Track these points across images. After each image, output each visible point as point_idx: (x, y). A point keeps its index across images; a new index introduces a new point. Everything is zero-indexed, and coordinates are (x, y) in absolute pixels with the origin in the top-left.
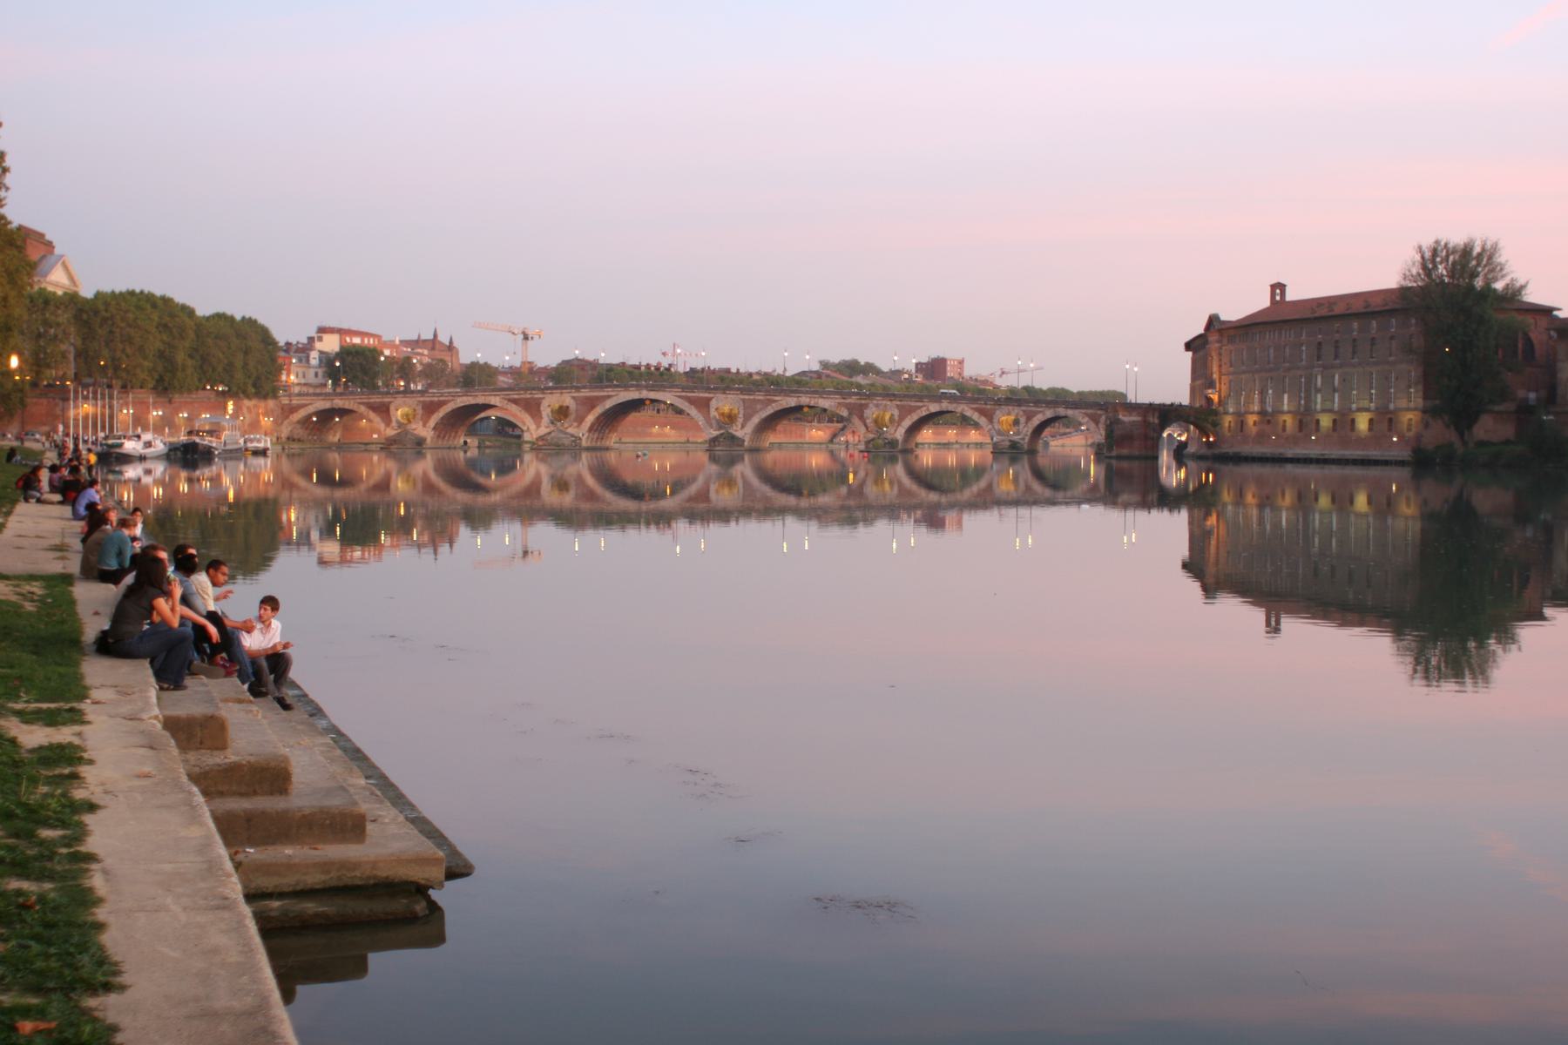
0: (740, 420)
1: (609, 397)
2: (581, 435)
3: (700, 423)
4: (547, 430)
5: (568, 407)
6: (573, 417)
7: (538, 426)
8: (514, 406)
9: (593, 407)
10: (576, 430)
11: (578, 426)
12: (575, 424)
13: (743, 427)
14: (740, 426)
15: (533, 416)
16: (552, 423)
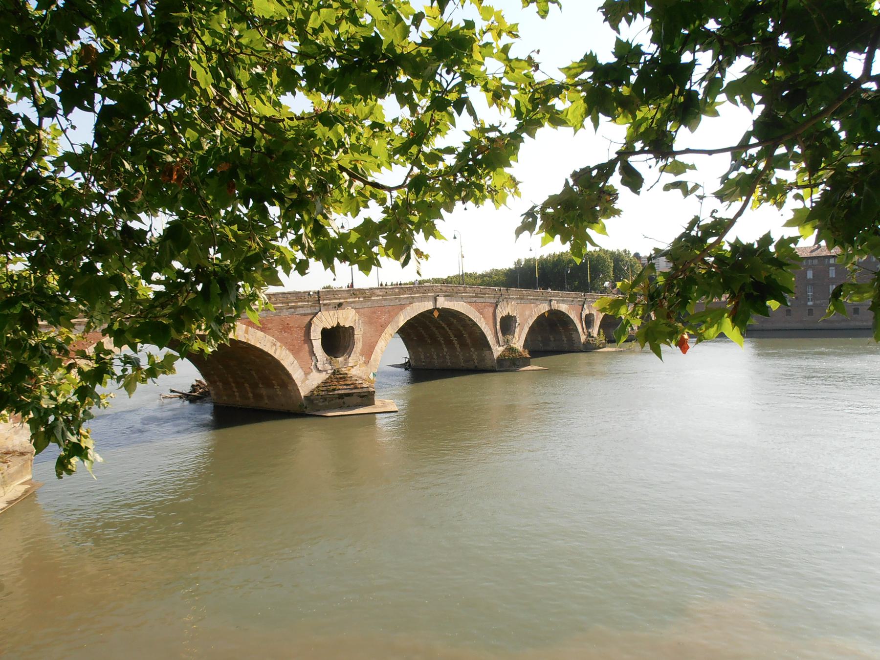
0: (517, 330)
1: (402, 307)
2: (371, 376)
3: (489, 339)
4: (324, 376)
5: (352, 328)
6: (358, 346)
7: (307, 374)
8: (260, 334)
9: (383, 327)
10: (363, 368)
11: (367, 363)
12: (363, 359)
13: (519, 337)
14: (518, 339)
15: (295, 352)
16: (330, 363)
